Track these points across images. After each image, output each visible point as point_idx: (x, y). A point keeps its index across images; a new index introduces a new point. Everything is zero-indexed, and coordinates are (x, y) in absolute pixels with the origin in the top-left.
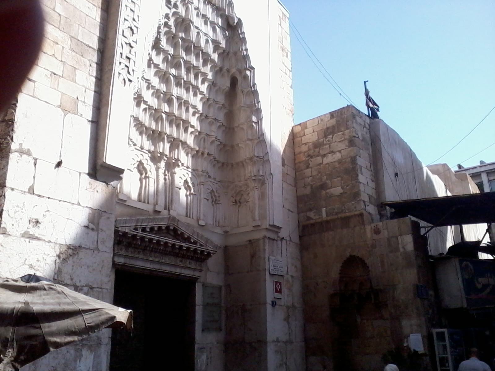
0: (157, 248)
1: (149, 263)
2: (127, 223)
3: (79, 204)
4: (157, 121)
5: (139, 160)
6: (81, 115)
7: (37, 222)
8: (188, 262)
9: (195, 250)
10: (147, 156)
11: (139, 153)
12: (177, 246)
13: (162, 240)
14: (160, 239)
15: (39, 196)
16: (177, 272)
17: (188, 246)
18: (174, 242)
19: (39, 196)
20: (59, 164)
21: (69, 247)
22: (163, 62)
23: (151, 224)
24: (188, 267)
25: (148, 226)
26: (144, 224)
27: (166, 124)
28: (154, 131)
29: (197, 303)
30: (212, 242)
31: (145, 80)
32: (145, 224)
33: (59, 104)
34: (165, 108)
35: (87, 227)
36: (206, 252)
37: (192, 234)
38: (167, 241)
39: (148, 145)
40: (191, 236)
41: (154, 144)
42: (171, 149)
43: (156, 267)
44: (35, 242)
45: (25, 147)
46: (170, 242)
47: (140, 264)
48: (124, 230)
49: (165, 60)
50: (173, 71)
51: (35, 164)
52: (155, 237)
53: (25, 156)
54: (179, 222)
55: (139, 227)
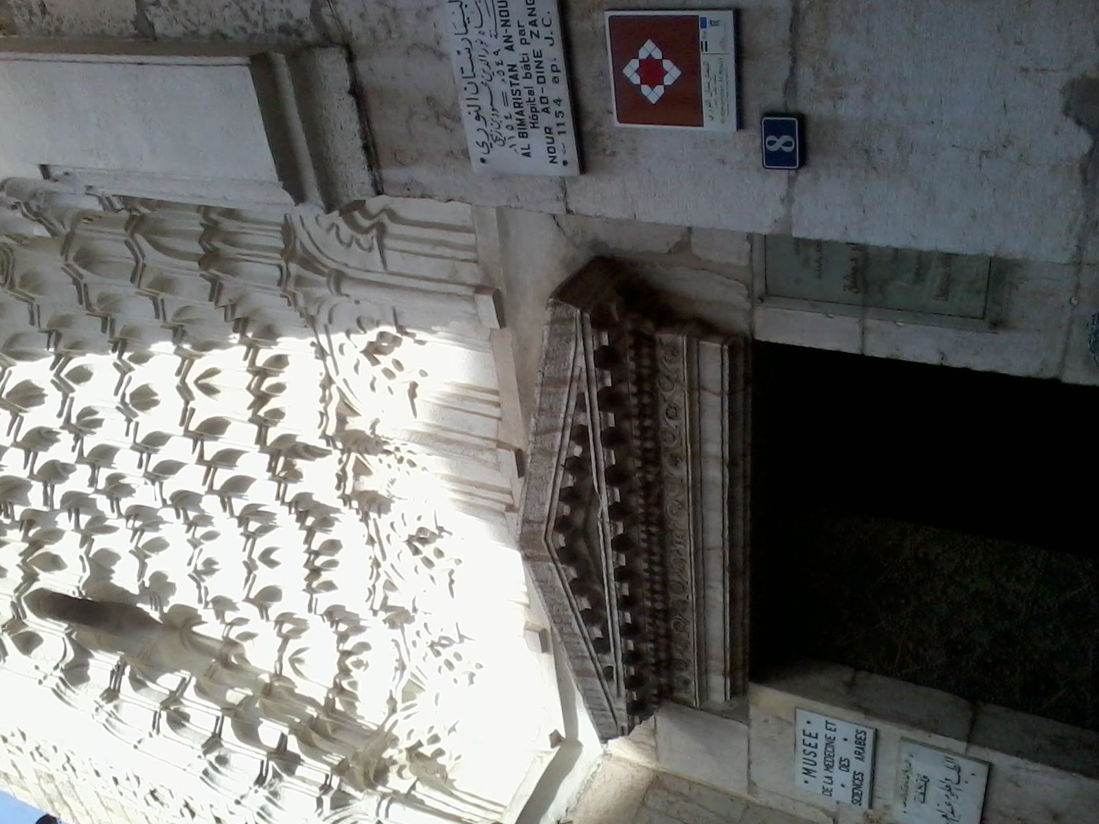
0: (647, 585)
1: (710, 593)
2: (601, 705)
5: (407, 551)
8: (672, 423)
12: (616, 529)
13: (613, 593)
14: (614, 601)
16: (719, 482)
17: (603, 485)
18: (610, 550)
24: (692, 430)
25: (587, 635)
29: (851, 348)
30: (550, 357)
31: (203, 584)
32: (584, 647)
34: (211, 505)
36: (602, 379)
37: (551, 455)
38: (612, 577)
40: (563, 462)
42: (311, 452)
43: (716, 569)
46: (611, 562)
47: (717, 626)
48: (624, 714)
49: (99, 525)
52: (615, 618)
54: (531, 518)
55: (598, 665)
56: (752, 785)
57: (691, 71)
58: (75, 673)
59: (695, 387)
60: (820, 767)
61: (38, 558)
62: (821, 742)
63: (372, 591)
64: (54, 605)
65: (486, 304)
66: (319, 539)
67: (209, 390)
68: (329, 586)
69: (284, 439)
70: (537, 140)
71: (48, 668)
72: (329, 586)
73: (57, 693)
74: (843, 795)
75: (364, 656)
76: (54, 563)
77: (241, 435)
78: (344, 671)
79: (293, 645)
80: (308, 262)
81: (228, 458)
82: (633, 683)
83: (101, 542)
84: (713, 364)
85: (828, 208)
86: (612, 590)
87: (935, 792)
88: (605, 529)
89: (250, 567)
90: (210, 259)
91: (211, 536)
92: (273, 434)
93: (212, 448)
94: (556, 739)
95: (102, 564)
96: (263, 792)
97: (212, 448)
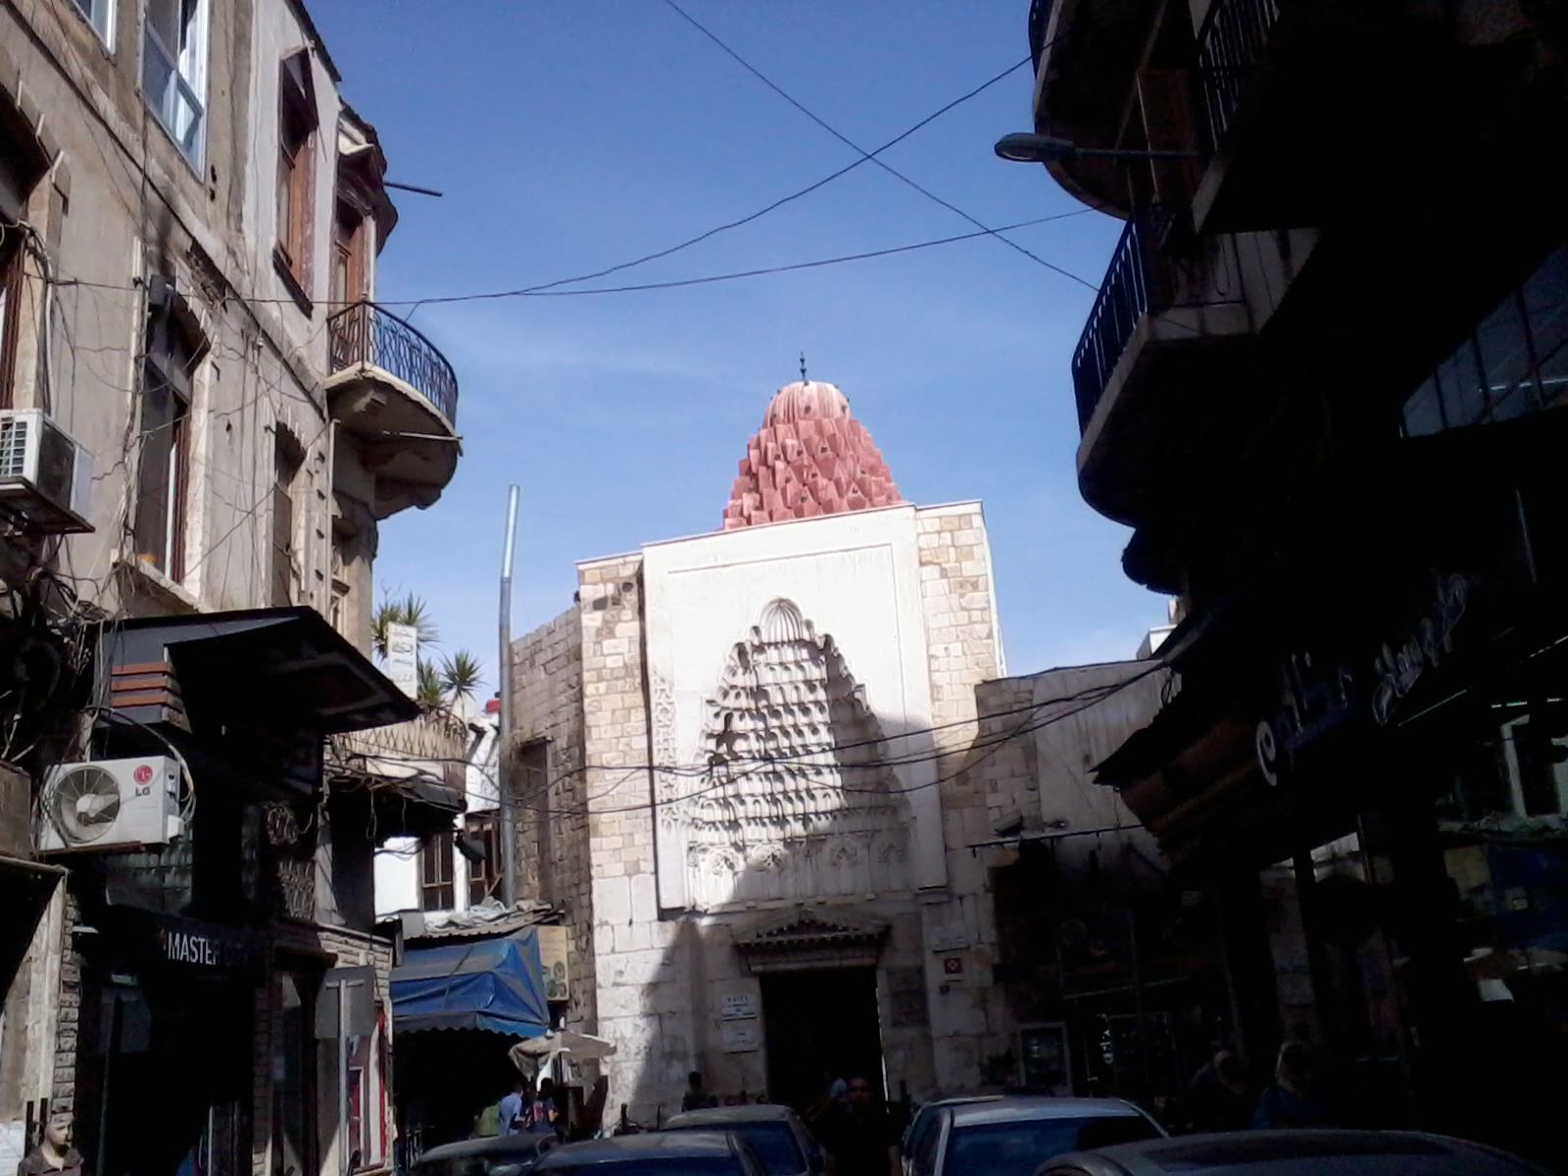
3: (653, 948)
4: (776, 805)
6: (644, 872)
7: (621, 973)
9: (847, 937)
10: (780, 846)
11: (768, 847)
15: (620, 953)
19: (620, 953)
20: (631, 922)
21: (650, 984)
22: (758, 740)
23: (777, 926)
26: (767, 930)
27: (785, 803)
28: (778, 817)
33: (623, 872)
34: (779, 787)
35: (663, 964)
39: (775, 832)
41: (782, 828)
42: (805, 825)
43: (806, 965)
44: (622, 989)
45: (604, 919)
47: (782, 967)
49: (759, 737)
50: (771, 745)
51: (613, 929)
53: (605, 928)
56: (712, 982)
57: (953, 972)
58: (710, 736)
59: (862, 957)
60: (732, 1003)
61: (744, 712)
62: (744, 1001)
63: (750, 840)
64: (728, 719)
65: (872, 896)
66: (766, 821)
67: (825, 796)
68: (749, 824)
69: (811, 820)
70: (937, 943)
71: (712, 727)
72: (749, 824)
73: (703, 731)
74: (726, 1011)
75: (713, 830)
76: (742, 717)
77: (811, 807)
78: (707, 823)
79: (713, 802)
80: (873, 836)
81: (801, 799)
82: (757, 944)
83: (752, 736)
84: (868, 961)
85: (933, 997)
86: (795, 937)
87: (741, 1038)
88: (816, 936)
89: (752, 795)
90: (870, 808)
91: (761, 780)
92: (812, 816)
93: (804, 794)
94: (706, 911)
95: (744, 736)
96: (689, 820)
97: (804, 794)
